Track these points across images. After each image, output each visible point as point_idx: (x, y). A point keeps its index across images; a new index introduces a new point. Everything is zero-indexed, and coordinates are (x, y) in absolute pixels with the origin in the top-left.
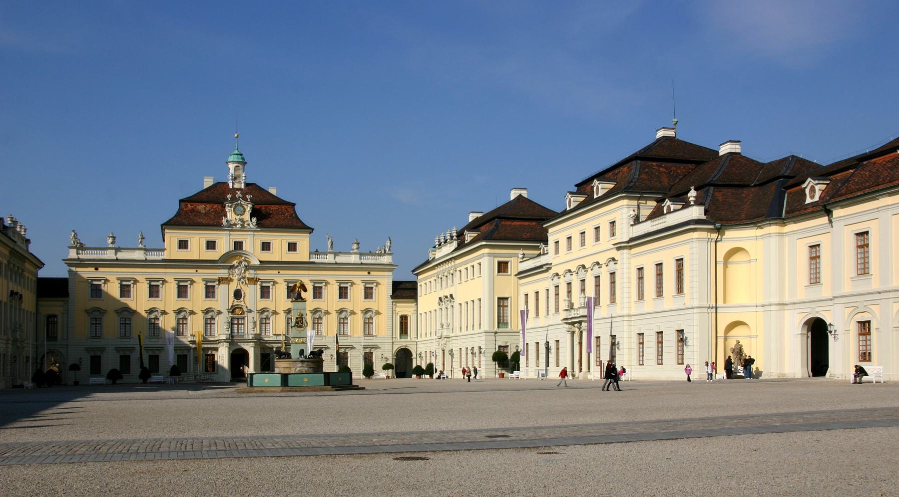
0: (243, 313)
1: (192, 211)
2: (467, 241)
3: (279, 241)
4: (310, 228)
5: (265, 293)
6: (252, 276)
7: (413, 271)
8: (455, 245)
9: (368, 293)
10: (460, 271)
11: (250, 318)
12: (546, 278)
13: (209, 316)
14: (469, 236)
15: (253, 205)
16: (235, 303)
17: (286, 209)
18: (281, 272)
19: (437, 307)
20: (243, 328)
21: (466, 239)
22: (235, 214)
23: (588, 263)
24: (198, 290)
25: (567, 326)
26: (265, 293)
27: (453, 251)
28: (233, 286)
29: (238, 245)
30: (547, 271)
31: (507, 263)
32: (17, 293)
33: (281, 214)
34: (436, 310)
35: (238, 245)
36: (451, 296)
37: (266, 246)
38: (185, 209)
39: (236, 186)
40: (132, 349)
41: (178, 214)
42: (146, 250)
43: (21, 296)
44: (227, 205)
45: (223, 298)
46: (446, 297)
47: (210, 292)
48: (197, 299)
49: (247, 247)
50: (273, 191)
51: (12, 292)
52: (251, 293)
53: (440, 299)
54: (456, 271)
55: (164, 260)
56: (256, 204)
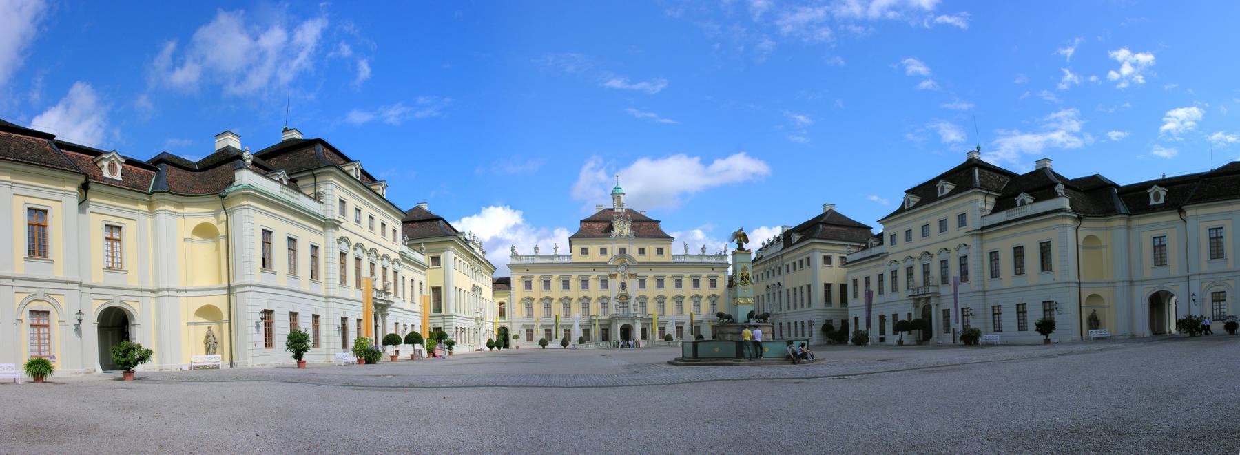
0: (627, 298)
1: (589, 228)
3: (651, 249)
5: (642, 284)
6: (631, 273)
8: (782, 245)
9: (713, 283)
10: (788, 266)
11: (632, 302)
12: (883, 265)
13: (604, 301)
14: (796, 237)
16: (620, 293)
18: (653, 269)
19: (764, 292)
23: (933, 250)
24: (594, 284)
25: (912, 302)
26: (642, 284)
27: (783, 249)
29: (622, 251)
30: (882, 258)
32: (477, 287)
34: (763, 296)
35: (622, 251)
36: (779, 283)
37: (642, 251)
39: (620, 210)
40: (552, 325)
41: (580, 231)
43: (480, 289)
46: (774, 285)
47: (604, 284)
48: (595, 290)
51: (474, 285)
52: (633, 285)
53: (768, 286)
54: (783, 265)
55: (570, 263)
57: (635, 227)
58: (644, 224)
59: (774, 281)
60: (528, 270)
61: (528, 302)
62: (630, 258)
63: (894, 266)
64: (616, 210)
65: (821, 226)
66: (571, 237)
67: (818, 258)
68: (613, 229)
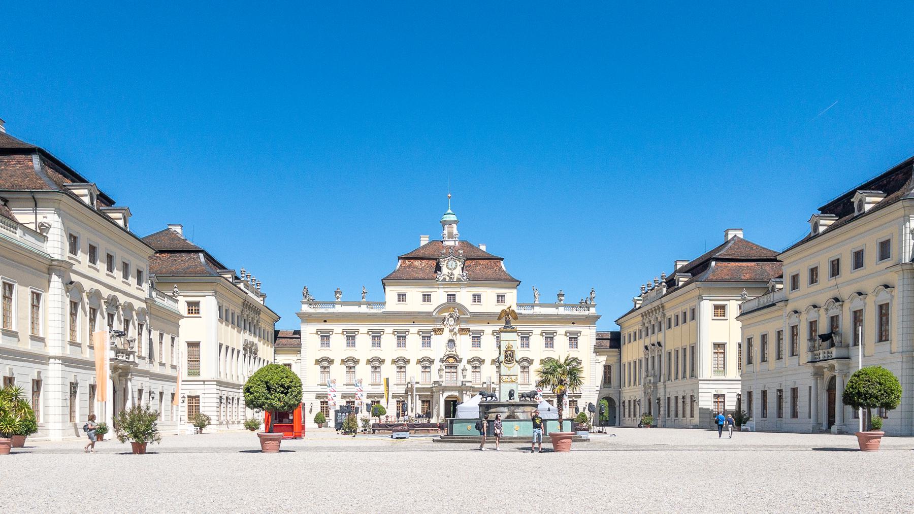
1: (410, 266)
2: (677, 285)
4: (518, 281)
7: (616, 321)
15: (464, 260)
16: (448, 353)
17: (495, 264)
20: (455, 376)
21: (676, 284)
22: (448, 268)
24: (414, 340)
28: (447, 335)
29: (452, 297)
31: (723, 307)
33: (490, 268)
35: (452, 297)
38: (403, 265)
42: (368, 304)
44: (441, 260)
45: (438, 347)
46: (653, 345)
48: (414, 348)
49: (458, 300)
50: (483, 248)
53: (646, 347)
56: (467, 259)
57: (469, 266)
58: (482, 262)
59: (654, 339)
60: (325, 321)
61: (325, 363)
62: (462, 308)
63: (794, 320)
64: (447, 243)
65: (713, 263)
66: (384, 279)
67: (707, 307)
68: (440, 270)
